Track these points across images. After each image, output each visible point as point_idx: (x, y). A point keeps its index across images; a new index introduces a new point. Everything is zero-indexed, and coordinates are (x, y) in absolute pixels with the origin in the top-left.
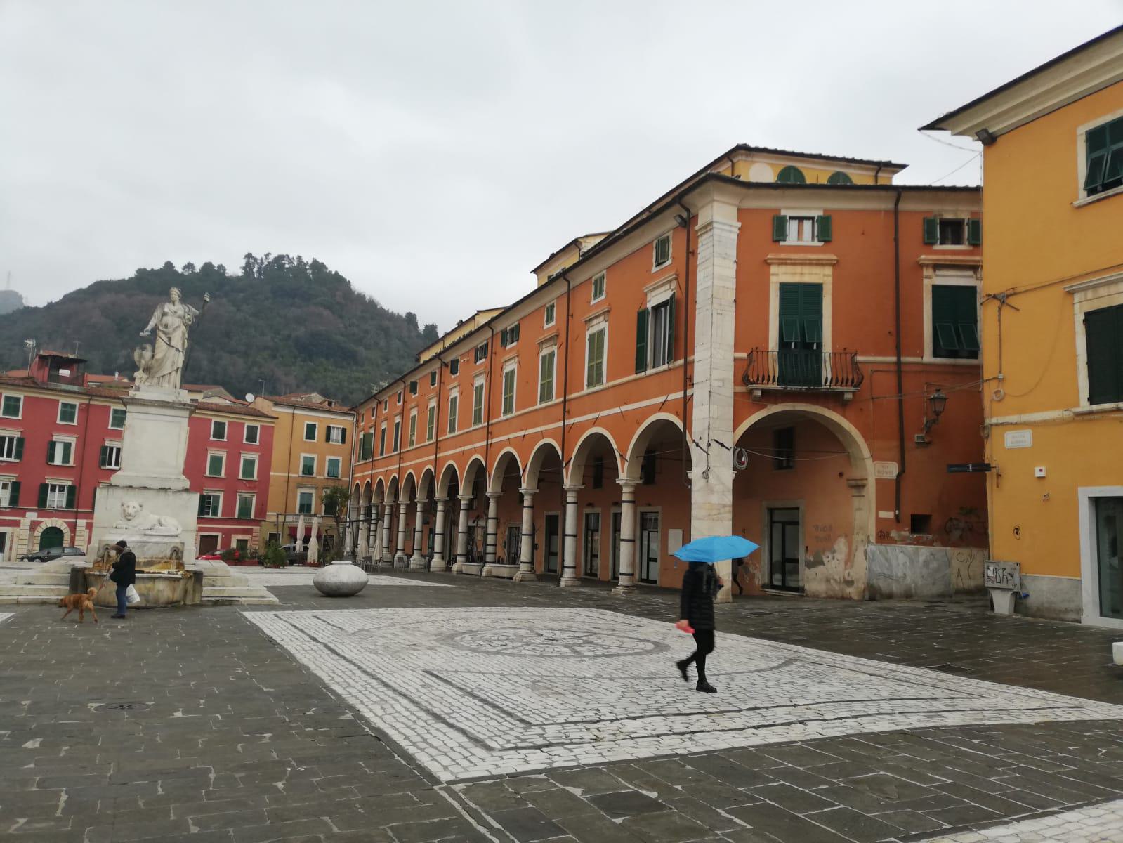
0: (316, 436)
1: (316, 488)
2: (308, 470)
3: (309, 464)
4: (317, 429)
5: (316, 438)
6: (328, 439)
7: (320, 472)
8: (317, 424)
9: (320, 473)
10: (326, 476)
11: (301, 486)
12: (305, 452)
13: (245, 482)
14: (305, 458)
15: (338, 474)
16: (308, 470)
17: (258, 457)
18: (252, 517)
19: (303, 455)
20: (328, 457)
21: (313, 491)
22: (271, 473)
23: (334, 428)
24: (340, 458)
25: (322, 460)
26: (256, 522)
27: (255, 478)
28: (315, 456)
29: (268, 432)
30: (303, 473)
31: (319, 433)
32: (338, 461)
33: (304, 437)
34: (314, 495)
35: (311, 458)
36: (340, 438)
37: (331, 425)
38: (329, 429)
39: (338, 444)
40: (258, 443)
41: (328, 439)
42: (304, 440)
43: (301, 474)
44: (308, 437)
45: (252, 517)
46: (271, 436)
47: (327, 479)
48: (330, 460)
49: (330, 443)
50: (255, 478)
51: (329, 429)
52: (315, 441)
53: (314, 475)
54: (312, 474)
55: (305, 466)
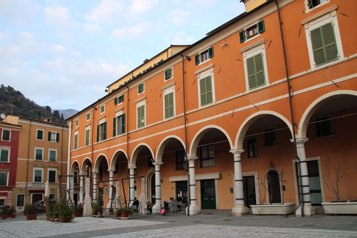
0: (43, 137)
1: (44, 167)
2: (39, 157)
3: (39, 153)
4: (43, 133)
5: (43, 139)
6: (49, 139)
7: (46, 158)
8: (43, 130)
9: (46, 159)
10: (49, 160)
11: (36, 166)
12: (37, 146)
13: (2, 164)
14: (37, 150)
15: (55, 159)
16: (39, 157)
17: (10, 149)
18: (7, 185)
19: (36, 148)
20: (50, 150)
21: (42, 169)
22: (18, 159)
23: (52, 133)
24: (56, 150)
25: (46, 151)
26: (10, 188)
27: (9, 161)
28: (43, 149)
29: (16, 134)
30: (37, 158)
31: (45, 135)
32: (55, 152)
33: (37, 138)
34: (43, 171)
35: (40, 150)
36: (56, 139)
37: (51, 132)
38: (50, 134)
39: (54, 142)
40: (10, 141)
41: (49, 139)
42: (37, 139)
43: (35, 159)
44: (38, 138)
45: (7, 185)
46: (18, 137)
47: (50, 162)
48: (51, 151)
49: (51, 141)
50: (9, 161)
51: (50, 134)
52: (43, 140)
53: (43, 160)
54: (41, 159)
55: (37, 155)
